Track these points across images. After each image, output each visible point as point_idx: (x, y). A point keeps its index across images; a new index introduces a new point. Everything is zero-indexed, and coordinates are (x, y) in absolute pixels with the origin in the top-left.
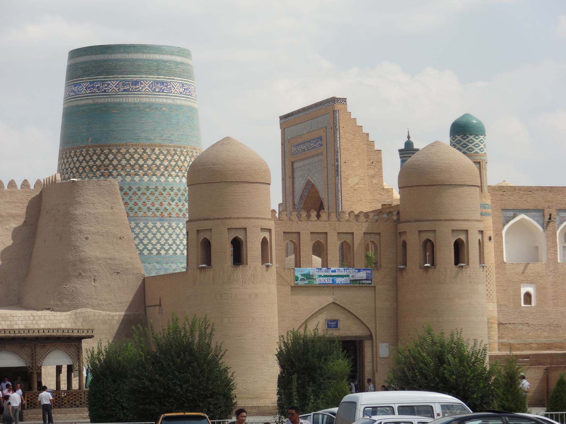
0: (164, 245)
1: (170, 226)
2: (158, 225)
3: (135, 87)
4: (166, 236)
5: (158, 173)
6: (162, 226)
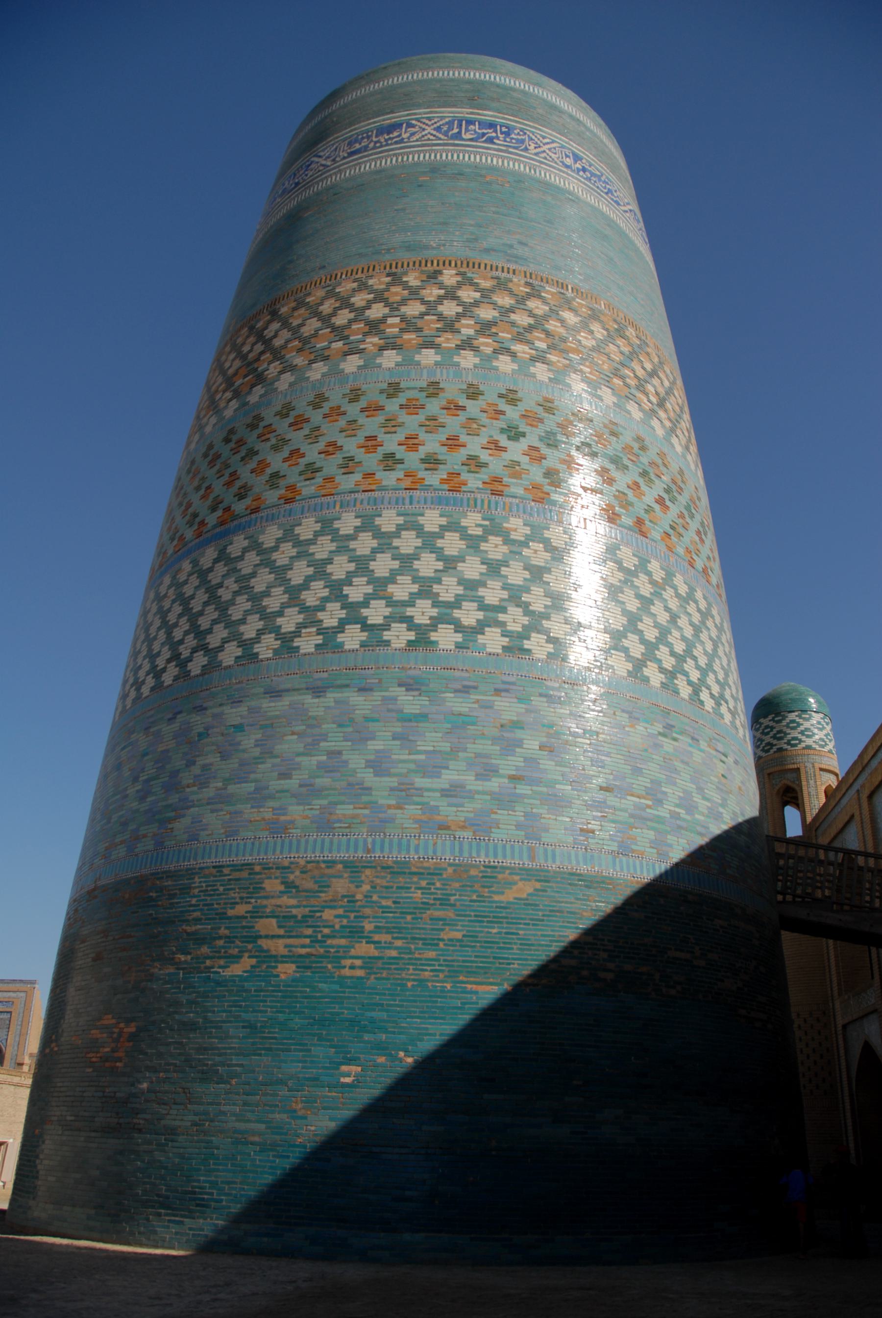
0: (457, 604)
1: (494, 529)
2: (432, 520)
3: (387, 137)
4: (472, 568)
5: (448, 341)
6: (453, 526)
